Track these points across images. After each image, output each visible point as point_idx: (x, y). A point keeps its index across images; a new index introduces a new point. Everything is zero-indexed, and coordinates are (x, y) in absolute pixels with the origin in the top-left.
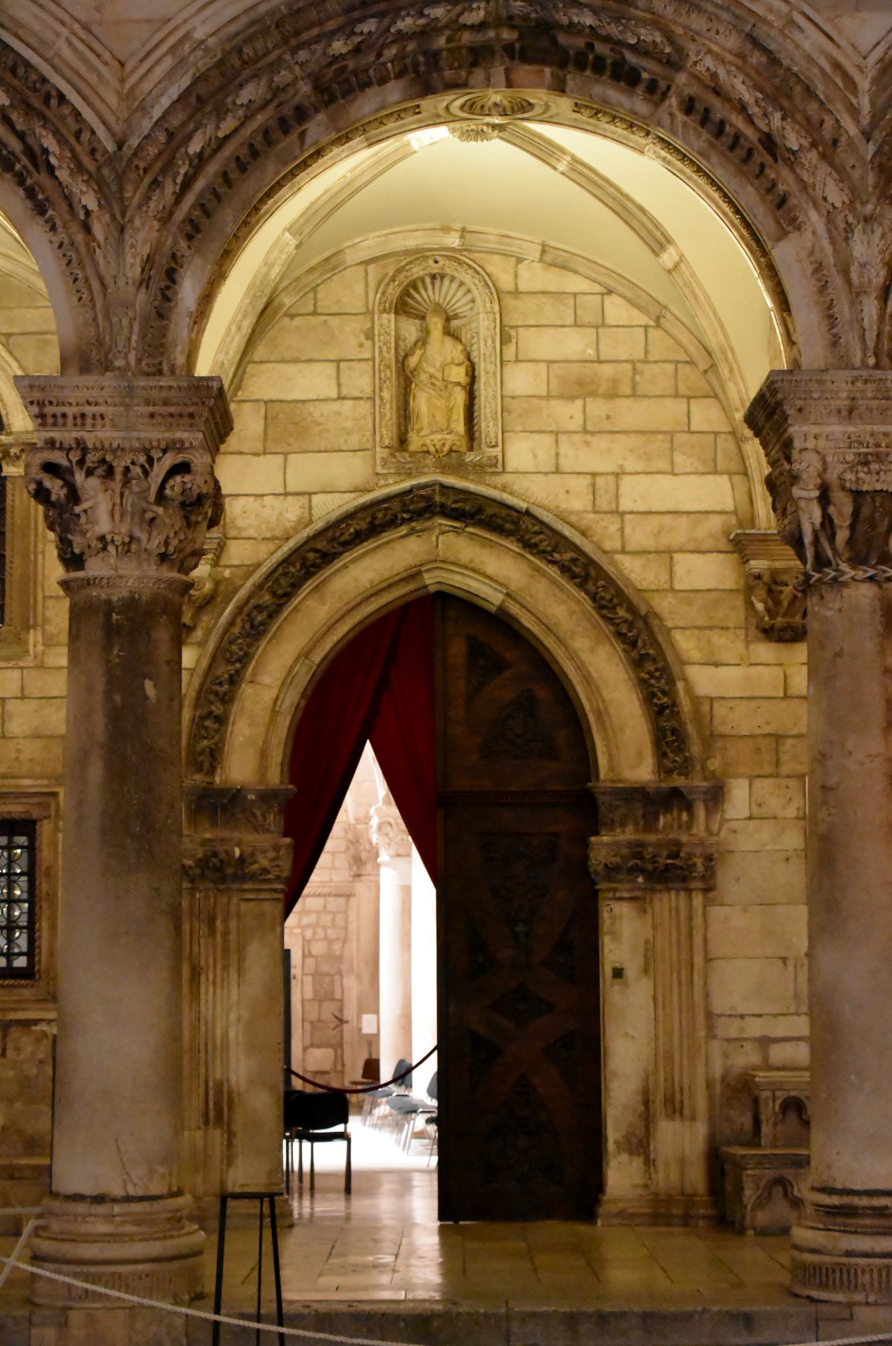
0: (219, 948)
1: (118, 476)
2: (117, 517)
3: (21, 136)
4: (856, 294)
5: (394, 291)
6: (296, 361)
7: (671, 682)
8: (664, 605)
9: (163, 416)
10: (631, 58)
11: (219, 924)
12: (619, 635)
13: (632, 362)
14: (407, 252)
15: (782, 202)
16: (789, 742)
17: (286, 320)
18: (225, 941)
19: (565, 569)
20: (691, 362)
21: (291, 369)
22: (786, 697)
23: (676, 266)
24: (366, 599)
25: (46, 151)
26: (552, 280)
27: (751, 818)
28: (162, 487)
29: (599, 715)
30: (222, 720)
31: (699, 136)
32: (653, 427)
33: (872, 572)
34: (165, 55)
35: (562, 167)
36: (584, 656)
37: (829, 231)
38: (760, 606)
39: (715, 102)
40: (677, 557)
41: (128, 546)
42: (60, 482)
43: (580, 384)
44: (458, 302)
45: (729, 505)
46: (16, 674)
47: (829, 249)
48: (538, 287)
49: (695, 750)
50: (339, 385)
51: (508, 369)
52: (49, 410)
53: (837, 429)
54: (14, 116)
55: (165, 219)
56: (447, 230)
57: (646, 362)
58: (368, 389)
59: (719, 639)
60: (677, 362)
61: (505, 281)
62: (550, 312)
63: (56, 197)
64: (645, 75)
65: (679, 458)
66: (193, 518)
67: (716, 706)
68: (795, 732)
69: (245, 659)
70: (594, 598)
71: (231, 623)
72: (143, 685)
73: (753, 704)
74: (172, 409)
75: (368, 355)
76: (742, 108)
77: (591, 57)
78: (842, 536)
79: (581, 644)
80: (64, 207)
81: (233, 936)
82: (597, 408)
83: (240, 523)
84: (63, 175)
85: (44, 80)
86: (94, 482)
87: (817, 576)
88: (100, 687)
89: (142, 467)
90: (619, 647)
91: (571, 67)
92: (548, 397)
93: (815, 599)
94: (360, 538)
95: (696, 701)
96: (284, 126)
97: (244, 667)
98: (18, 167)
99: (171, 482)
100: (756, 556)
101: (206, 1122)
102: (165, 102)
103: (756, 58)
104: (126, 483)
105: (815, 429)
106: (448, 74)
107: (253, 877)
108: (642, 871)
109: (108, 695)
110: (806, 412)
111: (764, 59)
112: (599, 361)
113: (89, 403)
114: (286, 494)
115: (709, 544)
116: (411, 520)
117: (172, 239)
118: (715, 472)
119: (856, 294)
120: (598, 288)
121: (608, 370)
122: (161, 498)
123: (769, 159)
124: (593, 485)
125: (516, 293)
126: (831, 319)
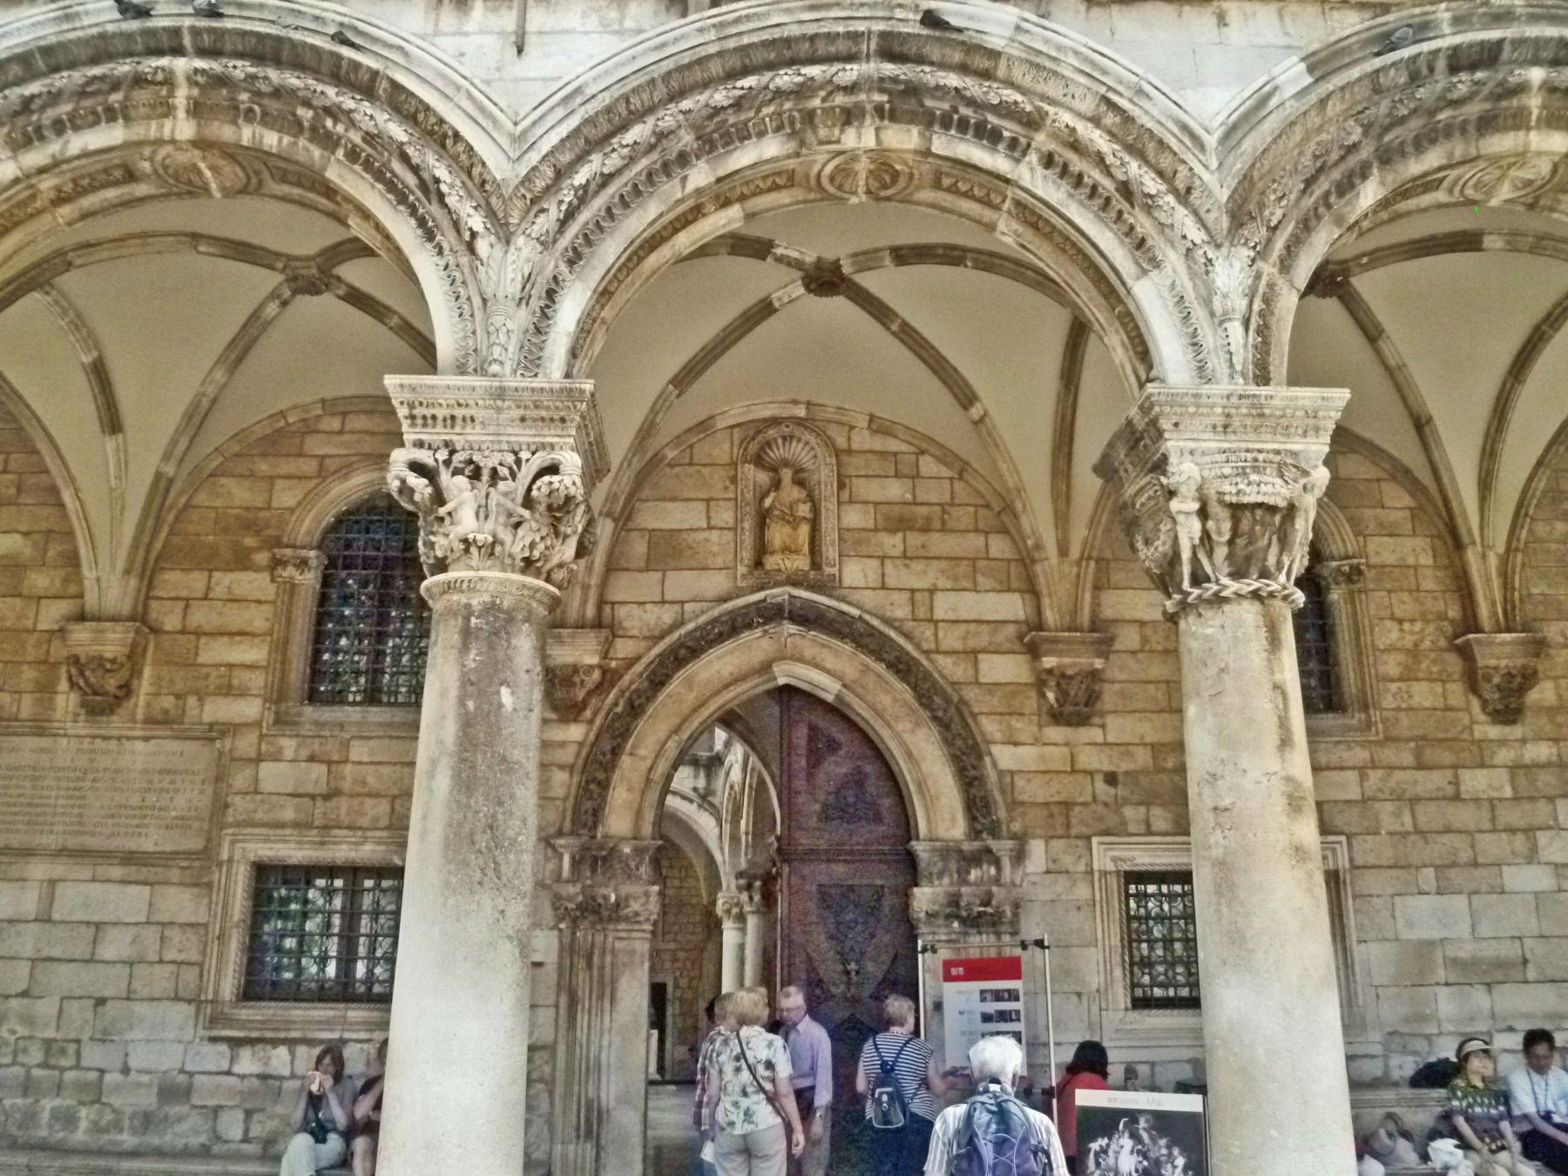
0: (595, 979)
1: (485, 477)
2: (482, 516)
3: (415, 170)
4: (1221, 320)
5: (753, 448)
6: (674, 499)
7: (980, 757)
8: (970, 694)
9: (534, 420)
10: (993, 120)
11: (596, 959)
12: (935, 718)
13: (941, 505)
14: (765, 420)
15: (1141, 244)
16: (1077, 809)
17: (668, 470)
18: (602, 976)
19: (890, 666)
20: (988, 506)
21: (670, 505)
22: (1074, 771)
23: (982, 420)
24: (727, 686)
25: (437, 181)
26: (877, 443)
27: (1048, 872)
28: (529, 489)
29: (920, 786)
30: (604, 786)
31: (1059, 187)
32: (960, 555)
33: (1256, 585)
34: (558, 105)
35: (895, 327)
36: (905, 736)
37: (1189, 268)
38: (1051, 696)
39: (1071, 156)
40: (981, 657)
41: (490, 549)
42: (425, 481)
43: (901, 520)
44: (805, 459)
45: (1021, 616)
47: (1189, 285)
48: (867, 447)
49: (1002, 813)
50: (709, 518)
51: (843, 508)
52: (418, 411)
53: (1212, 443)
54: (410, 151)
55: (546, 243)
56: (795, 402)
57: (952, 505)
58: (731, 523)
59: (1017, 723)
60: (976, 506)
61: (841, 442)
62: (876, 466)
63: (446, 224)
64: (1006, 134)
65: (980, 578)
66: (562, 529)
67: (1016, 778)
68: (1082, 799)
69: (625, 734)
70: (915, 689)
71: (616, 704)
72: (498, 693)
73: (1047, 777)
74: (544, 413)
75: (732, 495)
76: (1100, 160)
77: (956, 117)
78: (1221, 552)
80: (451, 234)
81: (608, 970)
82: (915, 539)
83: (626, 624)
84: (451, 201)
85: (442, 121)
86: (461, 480)
87: (1196, 592)
88: (454, 693)
89: (510, 469)
90: (935, 730)
91: (936, 128)
92: (876, 530)
93: (1191, 619)
94: (721, 638)
95: (1001, 774)
96: (666, 168)
97: (625, 740)
98: (411, 198)
99: (538, 483)
100: (1049, 653)
101: (578, 1137)
102: (554, 138)
103: (1110, 119)
105: (1192, 445)
106: (823, 132)
107: (627, 919)
108: (957, 917)
109: (462, 702)
110: (1181, 427)
111: (1118, 119)
112: (916, 504)
113: (459, 405)
114: (664, 602)
115: (1008, 646)
116: (765, 624)
117: (552, 263)
118: (1009, 590)
119: (1221, 320)
120: (913, 449)
121: (923, 510)
122: (528, 502)
123: (1125, 206)
124: (912, 598)
125: (849, 451)
126: (1196, 345)
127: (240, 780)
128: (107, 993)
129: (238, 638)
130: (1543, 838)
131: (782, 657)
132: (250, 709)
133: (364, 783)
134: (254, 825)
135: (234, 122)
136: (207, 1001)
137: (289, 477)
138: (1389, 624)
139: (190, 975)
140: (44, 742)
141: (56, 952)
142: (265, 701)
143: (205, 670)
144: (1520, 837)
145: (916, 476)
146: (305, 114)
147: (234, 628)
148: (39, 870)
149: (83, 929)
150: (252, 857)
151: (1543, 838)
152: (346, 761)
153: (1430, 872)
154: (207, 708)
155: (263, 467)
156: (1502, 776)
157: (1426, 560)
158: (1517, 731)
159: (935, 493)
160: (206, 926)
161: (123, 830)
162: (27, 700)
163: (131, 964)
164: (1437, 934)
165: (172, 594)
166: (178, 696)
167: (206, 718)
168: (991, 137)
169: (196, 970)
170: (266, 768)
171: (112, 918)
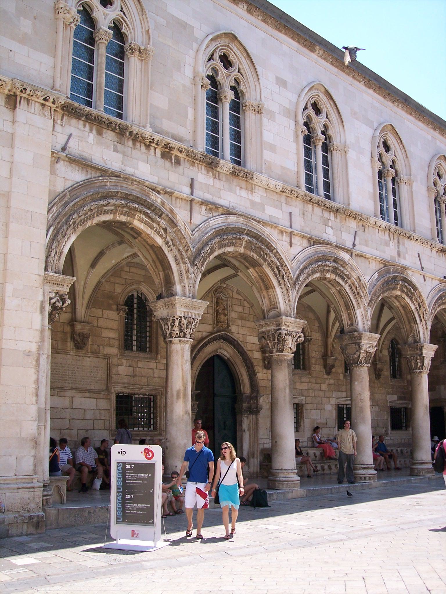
12: (246, 365)
38: (266, 363)
46: (155, 364)
76: (356, 288)
79: (240, 367)
82: (244, 322)
92: (237, 319)
104: (294, 337)
121: (245, 315)
127: (114, 370)
128: (89, 428)
129: (111, 330)
130: (331, 399)
131: (221, 348)
132: (114, 351)
133: (141, 373)
134: (118, 383)
135: (250, 251)
136: (112, 430)
137: (118, 284)
138: (314, 352)
139: (107, 423)
140: (64, 356)
141: (75, 417)
142: (118, 349)
143: (104, 339)
144: (328, 399)
145: (244, 306)
146: (262, 253)
147: (110, 327)
148: (68, 394)
149: (81, 410)
150: (117, 392)
151: (331, 399)
152: (137, 367)
153: (315, 405)
154: (105, 350)
155: (112, 279)
156: (326, 385)
157: (320, 339)
158: (329, 377)
159: (247, 311)
160: (110, 410)
161: (86, 383)
162: (60, 343)
163: (94, 420)
164: (316, 418)
165: (94, 315)
166: (98, 346)
167: (105, 353)
168: (343, 279)
169: (108, 422)
170: (121, 368)
171: (87, 408)
